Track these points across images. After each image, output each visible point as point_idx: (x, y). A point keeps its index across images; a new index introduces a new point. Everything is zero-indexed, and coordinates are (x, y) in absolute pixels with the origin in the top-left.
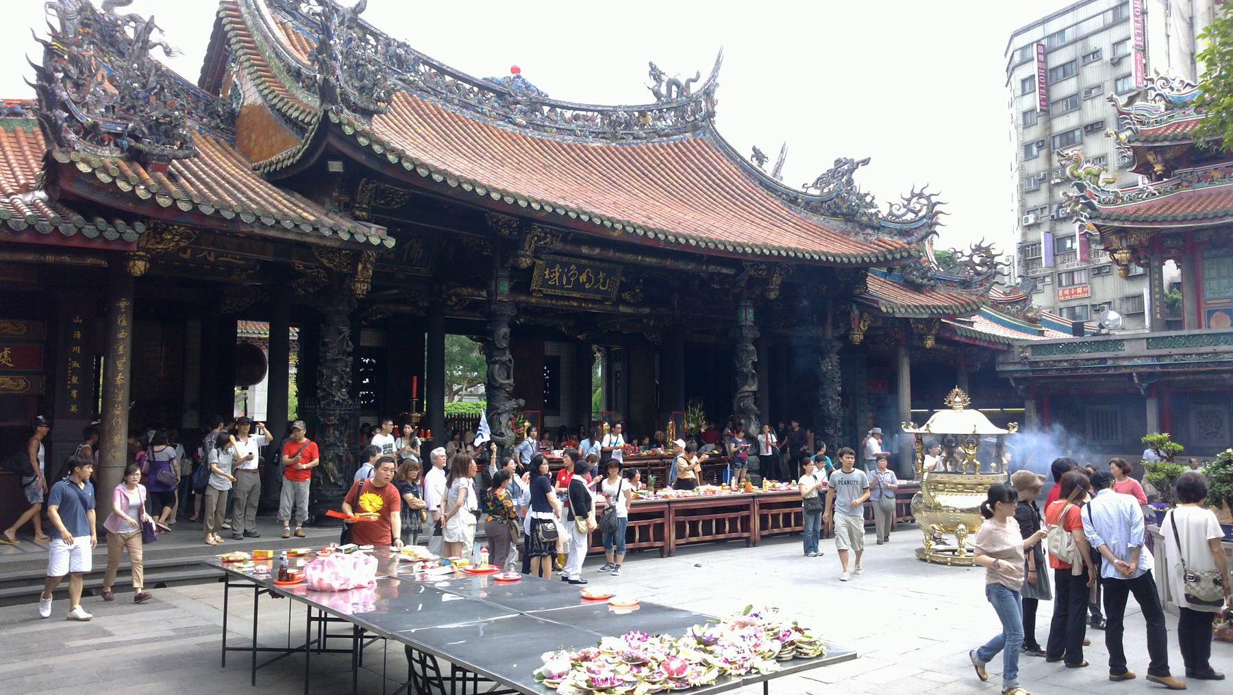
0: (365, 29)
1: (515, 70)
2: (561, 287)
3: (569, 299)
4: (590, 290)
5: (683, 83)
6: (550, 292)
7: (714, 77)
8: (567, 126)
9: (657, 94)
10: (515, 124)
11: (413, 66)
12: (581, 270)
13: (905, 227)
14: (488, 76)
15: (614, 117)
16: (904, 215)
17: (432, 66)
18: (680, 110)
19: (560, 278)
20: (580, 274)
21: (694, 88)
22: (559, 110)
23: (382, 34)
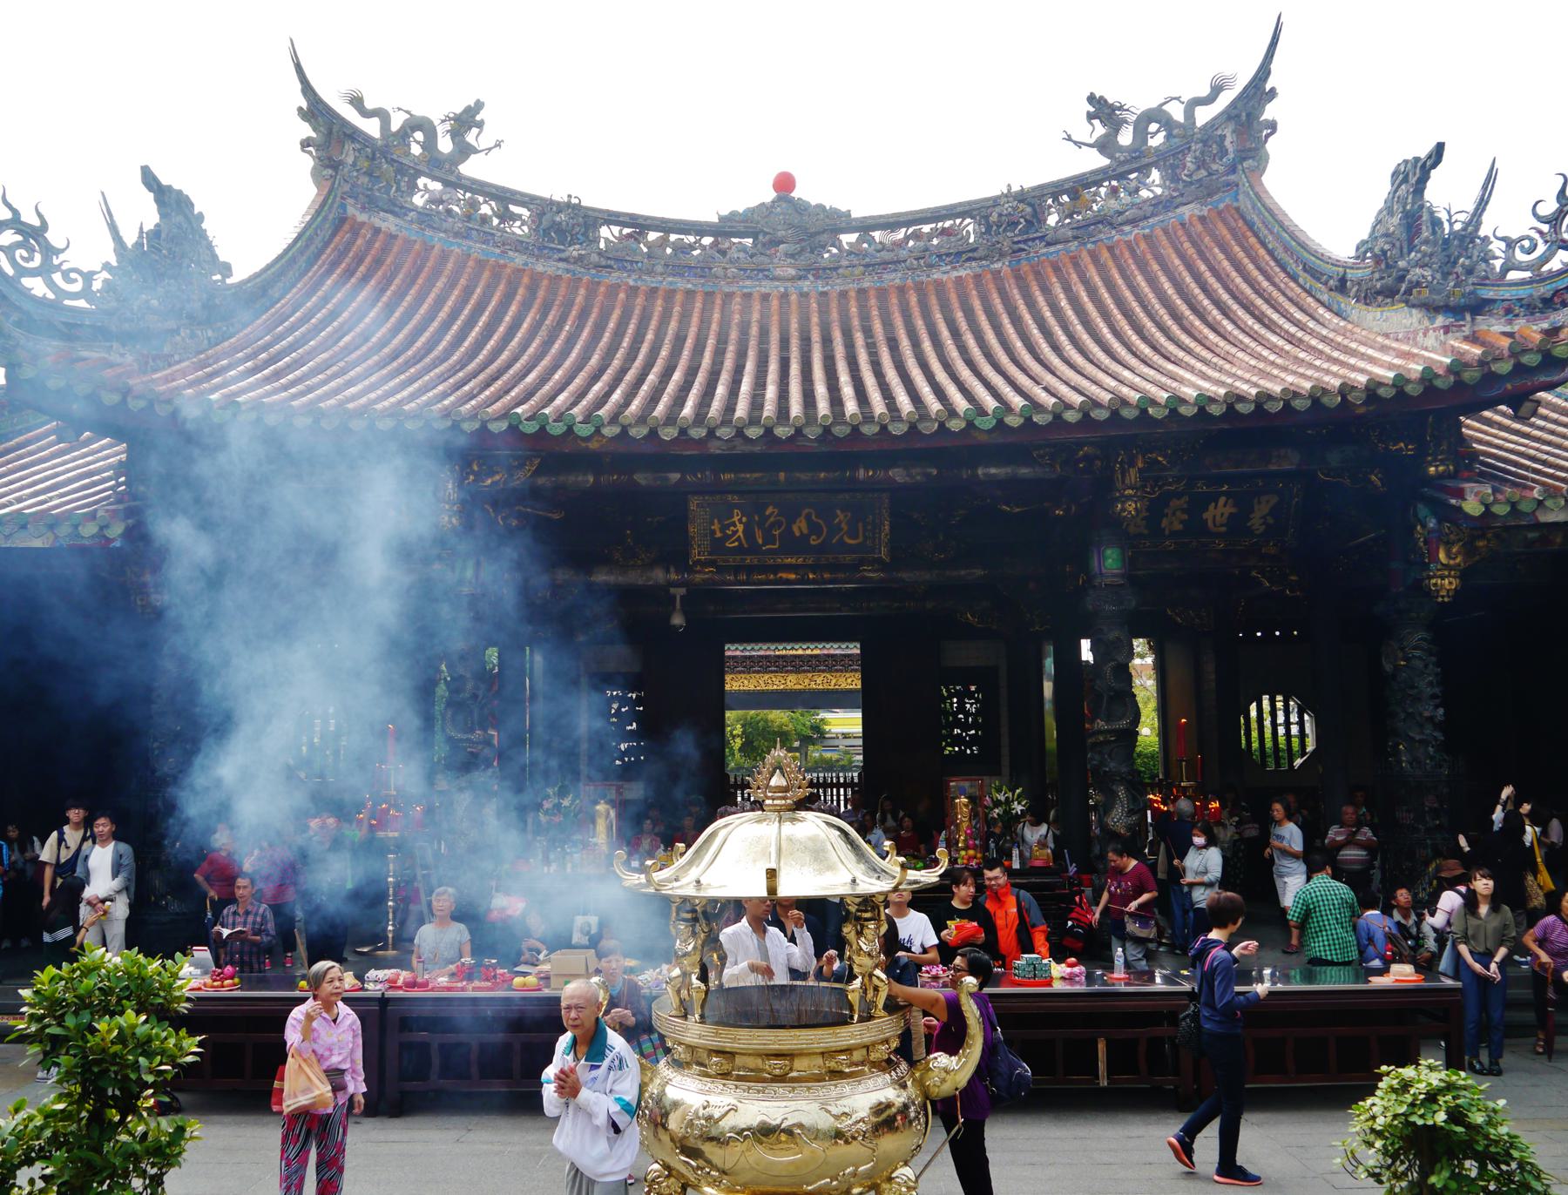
0: (504, 197)
2: (754, 549)
3: (776, 569)
4: (821, 549)
6: (732, 560)
8: (886, 255)
9: (1104, 146)
10: (775, 279)
11: (585, 234)
13: (1545, 290)
14: (725, 213)
15: (994, 218)
16: (1545, 259)
17: (623, 224)
18: (1168, 159)
19: (748, 531)
21: (1203, 115)
22: (877, 235)
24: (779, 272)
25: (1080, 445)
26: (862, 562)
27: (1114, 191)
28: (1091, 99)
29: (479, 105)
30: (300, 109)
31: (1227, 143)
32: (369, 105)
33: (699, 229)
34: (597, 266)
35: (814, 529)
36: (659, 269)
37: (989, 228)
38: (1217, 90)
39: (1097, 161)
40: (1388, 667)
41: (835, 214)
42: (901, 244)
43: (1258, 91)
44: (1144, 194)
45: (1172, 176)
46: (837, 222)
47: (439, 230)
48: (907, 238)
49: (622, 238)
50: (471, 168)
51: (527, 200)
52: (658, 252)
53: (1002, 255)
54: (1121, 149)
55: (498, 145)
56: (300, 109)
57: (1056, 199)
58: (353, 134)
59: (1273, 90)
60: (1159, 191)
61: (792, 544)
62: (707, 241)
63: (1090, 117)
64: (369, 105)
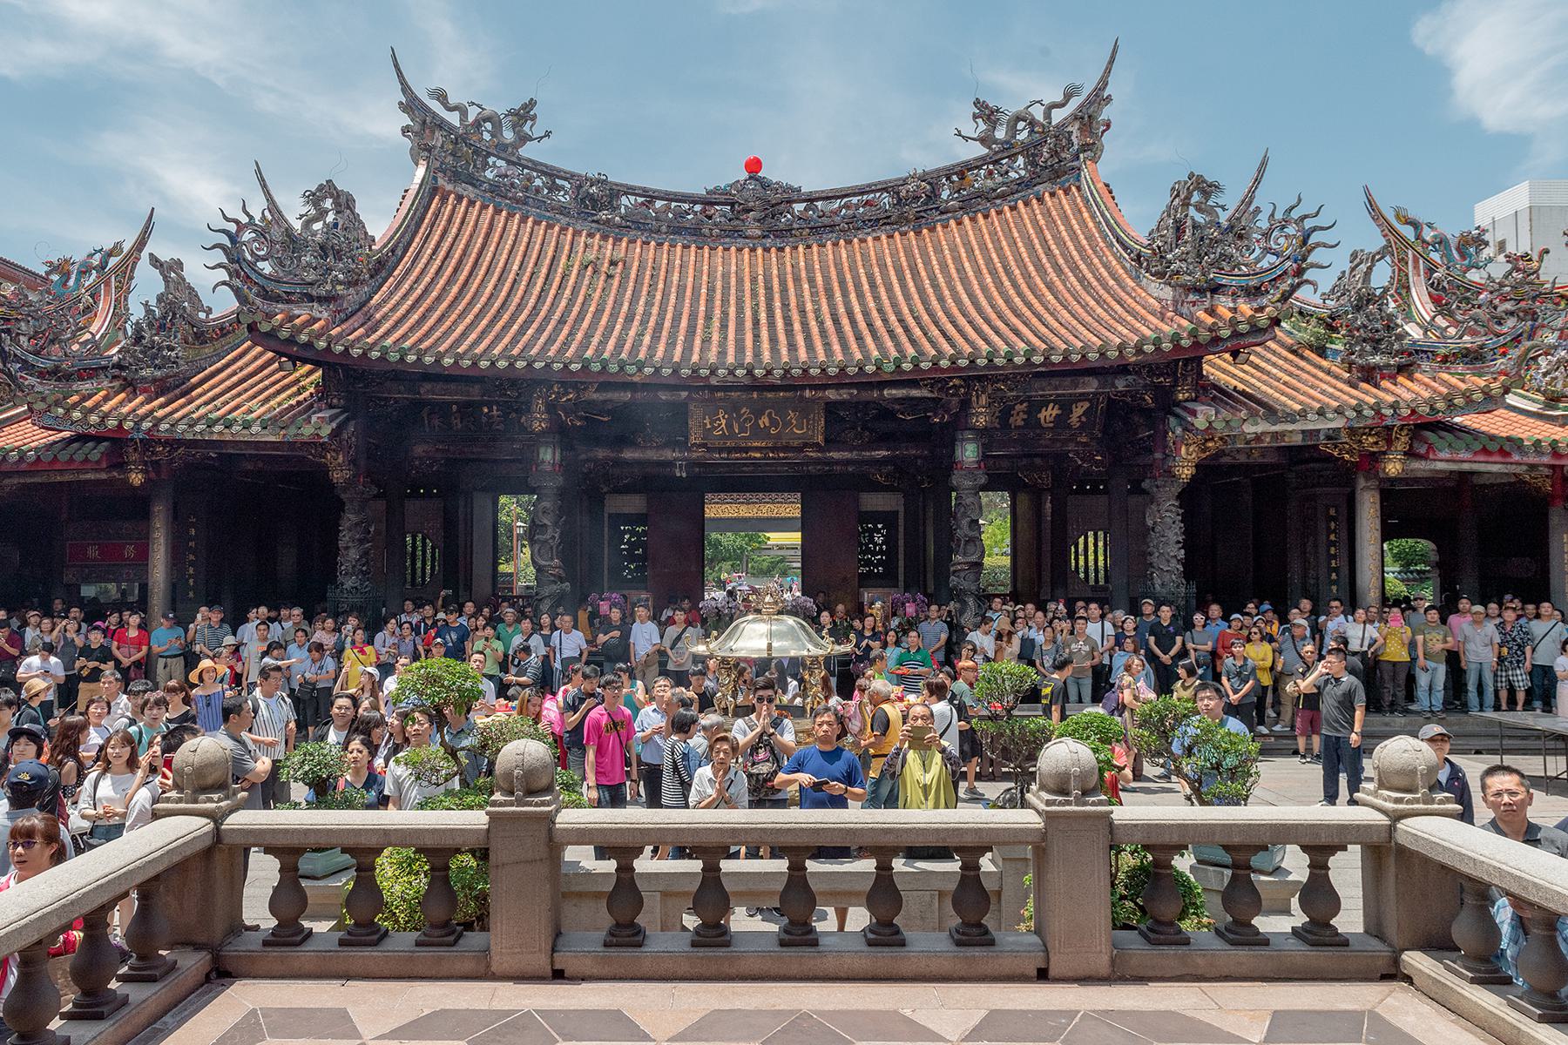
0: (551, 173)
1: (754, 166)
2: (732, 436)
3: (747, 450)
4: (778, 436)
5: (1038, 113)
7: (1103, 83)
8: (826, 221)
9: (984, 140)
12: (758, 414)
15: (903, 194)
16: (1258, 260)
18: (1031, 151)
19: (729, 426)
20: (758, 417)
21: (1058, 116)
23: (573, 175)
24: (749, 233)
25: (951, 378)
26: (806, 445)
27: (991, 173)
28: (977, 103)
29: (532, 103)
30: (401, 103)
31: (1073, 138)
32: (452, 101)
33: (694, 200)
34: (619, 227)
35: (774, 423)
36: (664, 229)
37: (900, 200)
38: (1068, 96)
39: (980, 150)
40: (1150, 523)
41: (790, 189)
42: (836, 213)
43: (1099, 97)
44: (1013, 175)
45: (1032, 162)
46: (790, 195)
47: (506, 197)
48: (841, 208)
49: (636, 205)
50: (528, 151)
51: (569, 177)
52: (663, 216)
53: (908, 221)
54: (996, 142)
55: (548, 134)
56: (401, 103)
57: (948, 178)
58: (441, 125)
59: (1109, 98)
60: (1023, 173)
61: (757, 432)
62: (698, 208)
63: (975, 117)
64: (452, 101)
